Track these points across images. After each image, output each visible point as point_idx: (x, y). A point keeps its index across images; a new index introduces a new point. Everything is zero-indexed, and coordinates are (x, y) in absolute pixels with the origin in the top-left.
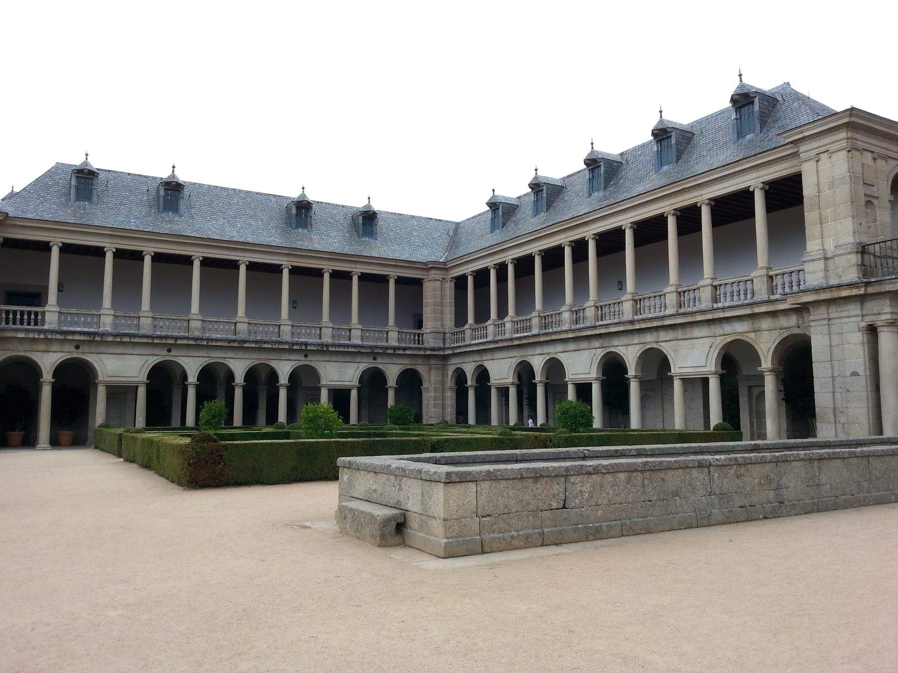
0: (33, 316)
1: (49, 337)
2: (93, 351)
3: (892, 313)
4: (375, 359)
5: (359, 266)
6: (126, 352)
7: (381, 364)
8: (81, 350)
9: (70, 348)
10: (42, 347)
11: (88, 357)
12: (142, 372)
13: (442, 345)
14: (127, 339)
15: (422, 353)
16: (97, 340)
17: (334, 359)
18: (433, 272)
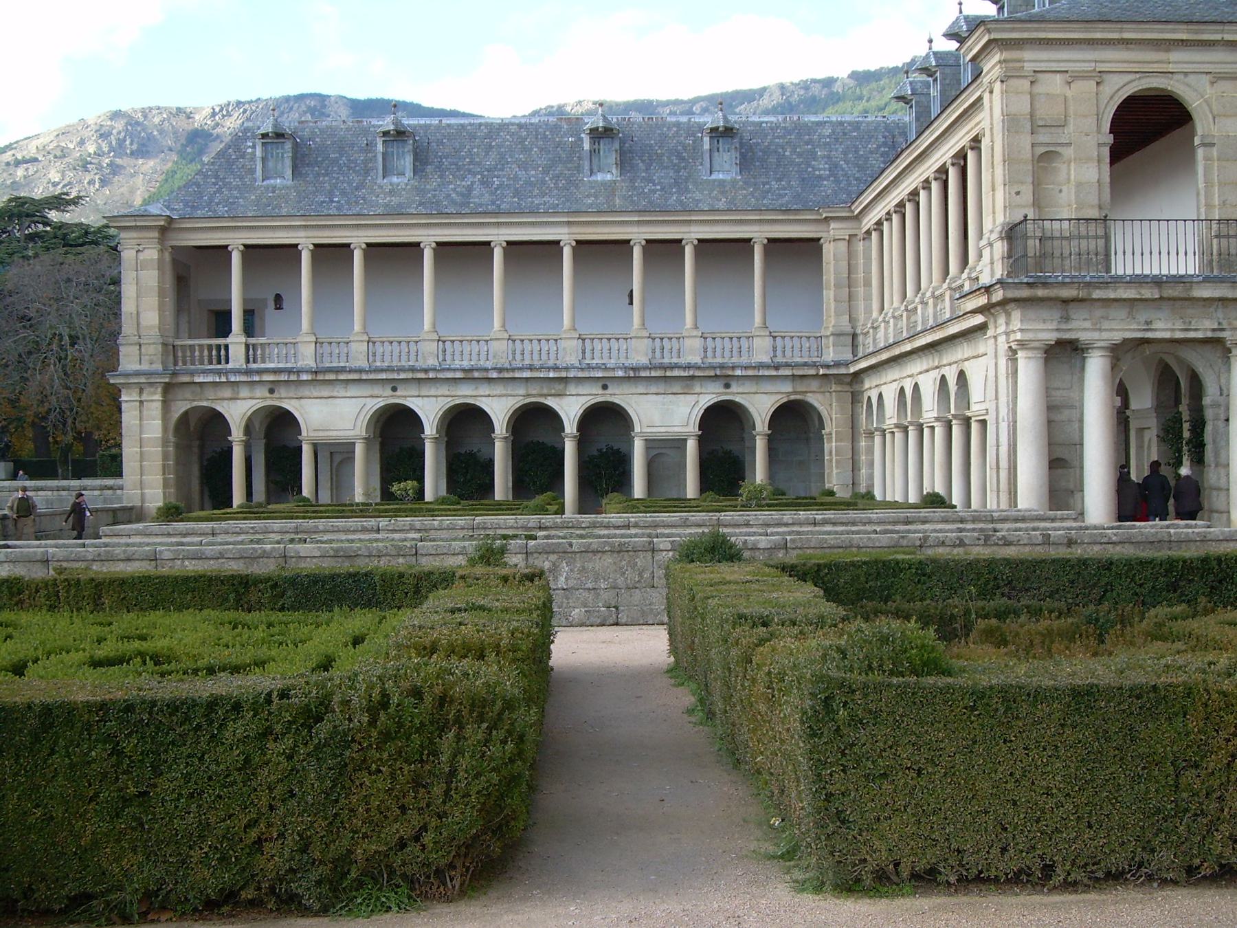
0: (214, 353)
1: (233, 379)
2: (291, 395)
3: (1021, 330)
4: (727, 386)
5: (693, 228)
6: (335, 394)
7: (738, 394)
8: (276, 395)
9: (262, 392)
10: (227, 393)
11: (286, 405)
12: (359, 423)
13: (849, 357)
14: (332, 377)
15: (812, 372)
16: (293, 379)
17: (653, 389)
18: (833, 225)
